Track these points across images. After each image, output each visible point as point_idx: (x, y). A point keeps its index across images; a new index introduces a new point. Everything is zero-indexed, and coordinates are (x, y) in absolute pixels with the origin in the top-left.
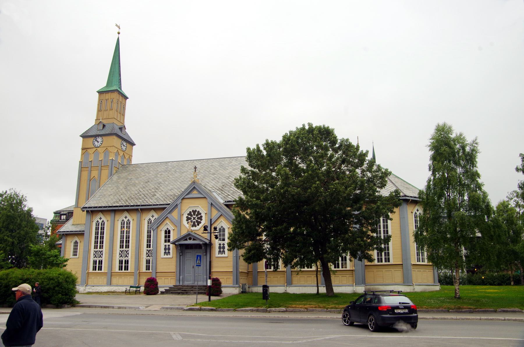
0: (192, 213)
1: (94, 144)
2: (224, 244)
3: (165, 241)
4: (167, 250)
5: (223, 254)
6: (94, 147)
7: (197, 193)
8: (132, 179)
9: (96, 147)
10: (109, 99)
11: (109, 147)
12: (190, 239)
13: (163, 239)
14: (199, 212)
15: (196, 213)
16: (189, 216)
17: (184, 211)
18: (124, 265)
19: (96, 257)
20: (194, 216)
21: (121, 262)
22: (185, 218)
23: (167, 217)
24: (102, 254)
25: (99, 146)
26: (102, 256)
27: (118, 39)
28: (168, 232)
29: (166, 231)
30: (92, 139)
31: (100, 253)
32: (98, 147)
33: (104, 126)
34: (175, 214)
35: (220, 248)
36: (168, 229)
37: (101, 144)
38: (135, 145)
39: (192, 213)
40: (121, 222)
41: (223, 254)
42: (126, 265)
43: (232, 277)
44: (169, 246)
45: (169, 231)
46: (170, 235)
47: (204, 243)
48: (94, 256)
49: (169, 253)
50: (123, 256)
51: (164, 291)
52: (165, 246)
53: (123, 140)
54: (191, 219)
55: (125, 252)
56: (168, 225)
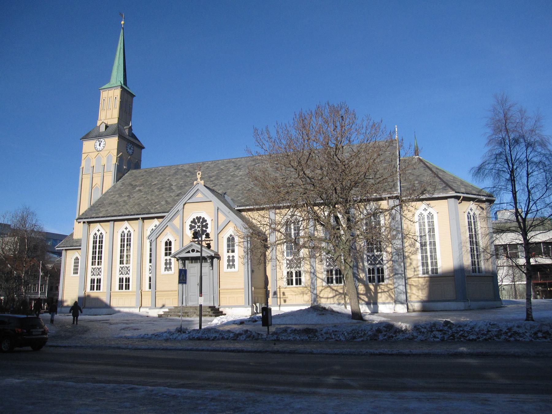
0: (196, 221)
1: (95, 148)
2: (233, 257)
3: (166, 255)
4: (168, 265)
5: (233, 268)
7: (202, 196)
8: (136, 185)
9: (98, 151)
10: (113, 97)
12: (193, 251)
13: (163, 252)
14: (204, 218)
15: (201, 220)
16: (193, 224)
17: (187, 219)
18: (124, 283)
19: (93, 274)
20: (199, 224)
21: (121, 280)
22: (187, 227)
23: (168, 226)
24: (101, 272)
25: (101, 149)
26: (100, 273)
28: (168, 244)
29: (166, 243)
31: (99, 270)
32: (101, 151)
33: (107, 127)
34: (177, 222)
35: (229, 261)
36: (168, 240)
37: (104, 147)
38: (144, 148)
39: (196, 221)
40: (121, 234)
41: (233, 268)
42: (121, 283)
43: (243, 295)
44: (170, 260)
45: (170, 243)
46: (171, 247)
47: (210, 255)
48: (92, 274)
49: (170, 268)
50: (123, 273)
51: (163, 313)
52: (166, 260)
53: (128, 143)
54: (195, 227)
55: (126, 269)
56: (168, 235)
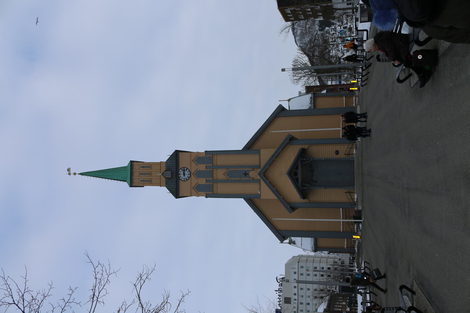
1: (187, 180)
9: (190, 176)
11: (191, 159)
25: (189, 173)
27: (82, 174)
30: (182, 184)
32: (190, 173)
37: (186, 170)
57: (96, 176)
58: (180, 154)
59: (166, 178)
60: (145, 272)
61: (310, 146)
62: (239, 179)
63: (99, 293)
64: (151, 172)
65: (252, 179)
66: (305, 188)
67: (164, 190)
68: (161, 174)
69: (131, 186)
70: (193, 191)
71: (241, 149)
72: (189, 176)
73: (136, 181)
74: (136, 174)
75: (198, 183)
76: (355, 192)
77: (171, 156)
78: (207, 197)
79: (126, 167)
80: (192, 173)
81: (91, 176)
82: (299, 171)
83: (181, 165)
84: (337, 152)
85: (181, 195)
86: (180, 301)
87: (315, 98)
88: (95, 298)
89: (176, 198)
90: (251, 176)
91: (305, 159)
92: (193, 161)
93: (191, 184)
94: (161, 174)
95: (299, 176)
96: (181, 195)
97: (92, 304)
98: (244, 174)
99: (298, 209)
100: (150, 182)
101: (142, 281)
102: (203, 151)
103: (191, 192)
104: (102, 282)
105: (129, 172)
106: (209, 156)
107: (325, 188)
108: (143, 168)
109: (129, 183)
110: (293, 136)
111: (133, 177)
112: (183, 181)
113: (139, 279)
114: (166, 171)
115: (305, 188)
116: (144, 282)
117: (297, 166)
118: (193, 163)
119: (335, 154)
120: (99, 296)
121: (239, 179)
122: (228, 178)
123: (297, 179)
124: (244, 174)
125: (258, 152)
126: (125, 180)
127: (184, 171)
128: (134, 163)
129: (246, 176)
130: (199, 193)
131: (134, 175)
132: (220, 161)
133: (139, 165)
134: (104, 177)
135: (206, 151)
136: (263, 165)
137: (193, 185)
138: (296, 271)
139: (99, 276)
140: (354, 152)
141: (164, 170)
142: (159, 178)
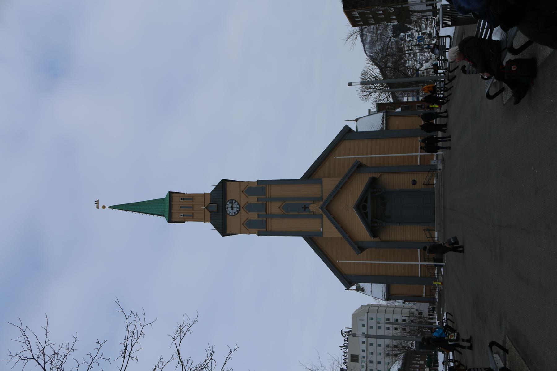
1: (236, 214)
6: (239, 213)
9: (240, 210)
11: (240, 189)
25: (238, 206)
27: (112, 207)
30: (229, 220)
32: (240, 206)
37: (235, 203)
57: (129, 210)
58: (228, 183)
59: (211, 212)
60: (186, 323)
61: (381, 174)
62: (297, 213)
63: (132, 347)
64: (193, 205)
65: (312, 213)
66: (376, 224)
67: (208, 227)
68: (205, 208)
69: (170, 221)
70: (243, 228)
71: (299, 178)
72: (238, 209)
73: (175, 216)
74: (175, 207)
75: (249, 219)
76: (435, 229)
77: (217, 186)
78: (259, 235)
79: (163, 199)
80: (242, 206)
81: (123, 210)
82: (369, 205)
83: (229, 196)
84: (414, 182)
85: (228, 232)
86: (227, 358)
87: (388, 118)
88: (127, 354)
89: (223, 235)
90: (311, 210)
91: (375, 190)
92: (242, 192)
93: (240, 219)
94: (205, 208)
95: (369, 210)
96: (228, 232)
97: (124, 360)
98: (303, 208)
99: (367, 250)
100: (192, 217)
101: (182, 334)
102: (254, 180)
103: (240, 229)
104: (136, 334)
105: (168, 204)
106: (261, 186)
107: (399, 225)
108: (184, 201)
109: (168, 218)
110: (362, 162)
111: (172, 211)
112: (230, 215)
113: (179, 331)
114: (210, 203)
115: (376, 224)
116: (185, 335)
117: (366, 199)
118: (242, 195)
119: (411, 185)
120: (131, 351)
121: (297, 213)
122: (285, 212)
123: (366, 214)
124: (303, 208)
125: (320, 182)
126: (162, 214)
127: (232, 203)
128: (174, 195)
129: (305, 210)
130: (250, 230)
131: (173, 209)
132: (275, 192)
133: (179, 197)
134: (138, 211)
135: (258, 181)
136: (325, 196)
137: (242, 221)
138: (365, 323)
139: (131, 328)
140: (435, 182)
141: (209, 203)
142: (203, 212)
